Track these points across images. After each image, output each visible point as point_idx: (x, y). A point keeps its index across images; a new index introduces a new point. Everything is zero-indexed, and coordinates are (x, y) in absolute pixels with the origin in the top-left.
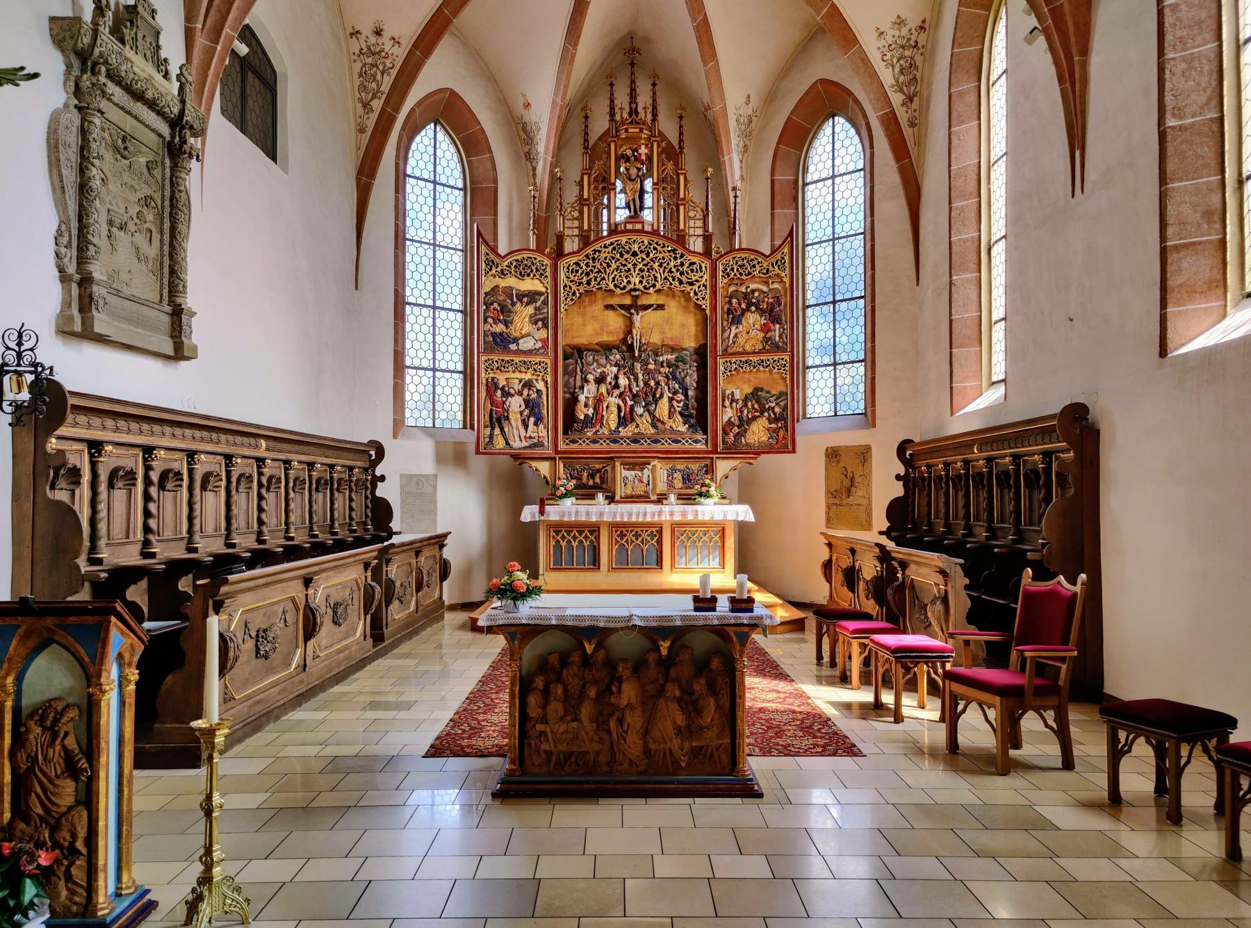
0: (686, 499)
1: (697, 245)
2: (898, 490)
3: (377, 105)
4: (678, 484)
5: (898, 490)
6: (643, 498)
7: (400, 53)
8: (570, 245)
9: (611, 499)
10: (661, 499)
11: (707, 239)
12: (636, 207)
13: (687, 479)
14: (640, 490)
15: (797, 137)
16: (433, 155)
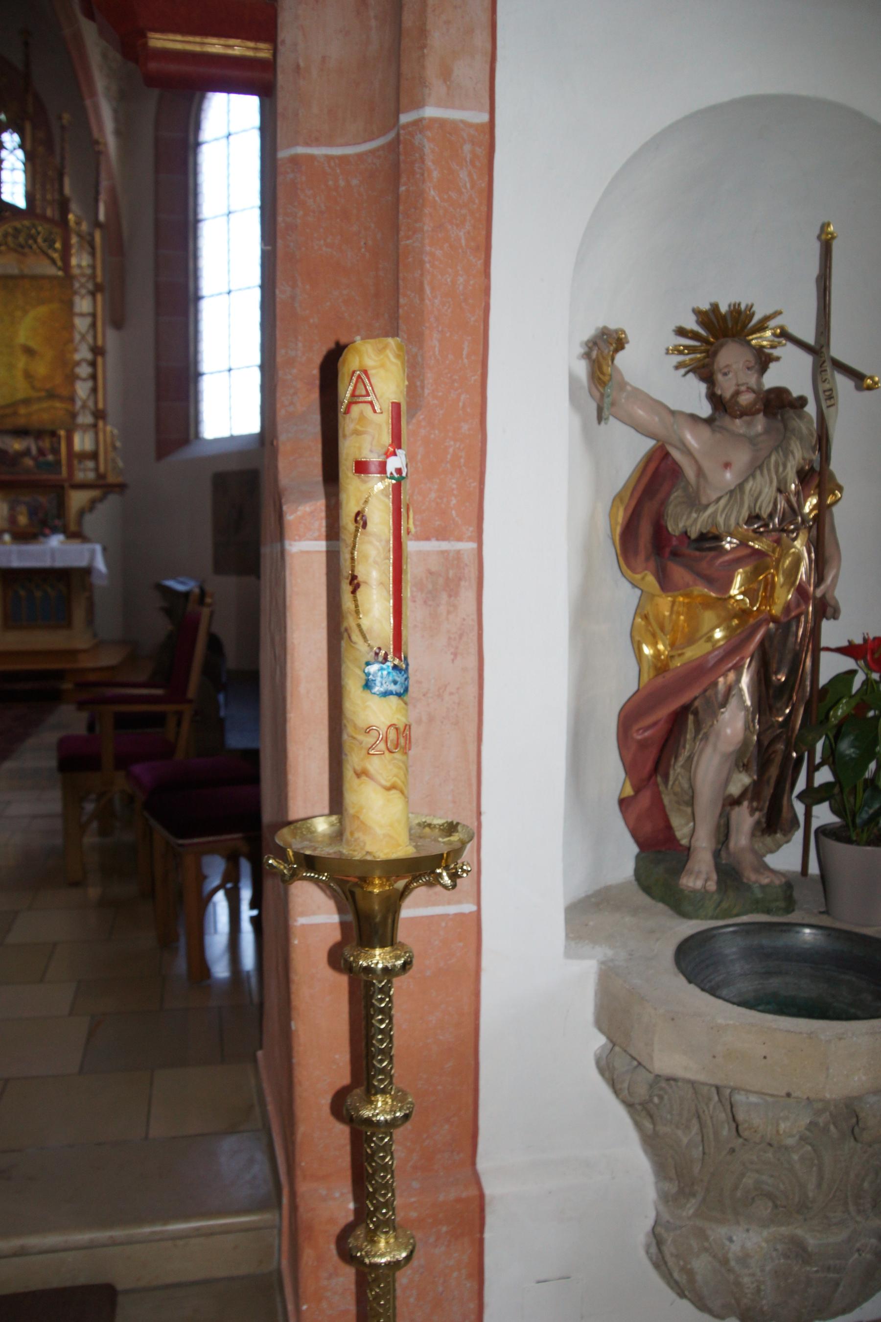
0: (22, 536)
4: (23, 520)
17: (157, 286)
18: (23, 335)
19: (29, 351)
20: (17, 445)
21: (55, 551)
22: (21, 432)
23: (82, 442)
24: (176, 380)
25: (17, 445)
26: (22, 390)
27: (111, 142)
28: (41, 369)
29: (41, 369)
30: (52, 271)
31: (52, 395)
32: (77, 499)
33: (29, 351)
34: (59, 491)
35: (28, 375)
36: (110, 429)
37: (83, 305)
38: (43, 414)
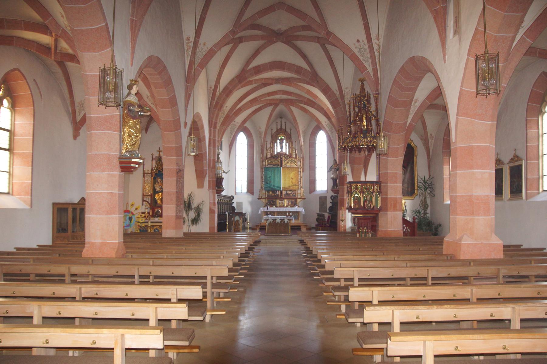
0: (291, 206)
1: (294, 156)
2: (331, 205)
3: (233, 133)
5: (331, 205)
6: (283, 206)
7: (238, 125)
8: (269, 156)
9: (277, 206)
10: (287, 206)
11: (296, 155)
12: (282, 147)
13: (292, 203)
14: (282, 205)
15: (314, 134)
16: (242, 139)
17: (310, 166)
18: (291, 176)
19: (292, 178)
20: (290, 192)
21: (296, 209)
22: (290, 191)
23: (299, 192)
24: (312, 182)
25: (290, 192)
26: (291, 184)
27: (303, 144)
28: (294, 181)
29: (294, 181)
30: (295, 166)
31: (295, 185)
32: (298, 200)
33: (292, 178)
34: (296, 199)
35: (292, 182)
36: (303, 189)
37: (299, 170)
38: (294, 188)
